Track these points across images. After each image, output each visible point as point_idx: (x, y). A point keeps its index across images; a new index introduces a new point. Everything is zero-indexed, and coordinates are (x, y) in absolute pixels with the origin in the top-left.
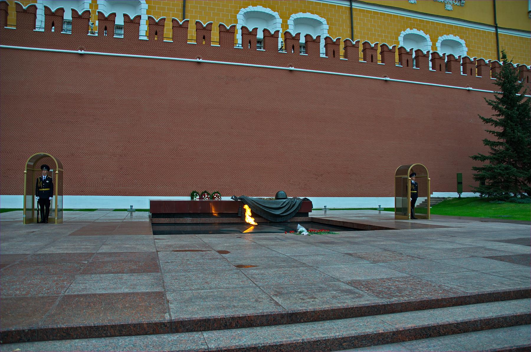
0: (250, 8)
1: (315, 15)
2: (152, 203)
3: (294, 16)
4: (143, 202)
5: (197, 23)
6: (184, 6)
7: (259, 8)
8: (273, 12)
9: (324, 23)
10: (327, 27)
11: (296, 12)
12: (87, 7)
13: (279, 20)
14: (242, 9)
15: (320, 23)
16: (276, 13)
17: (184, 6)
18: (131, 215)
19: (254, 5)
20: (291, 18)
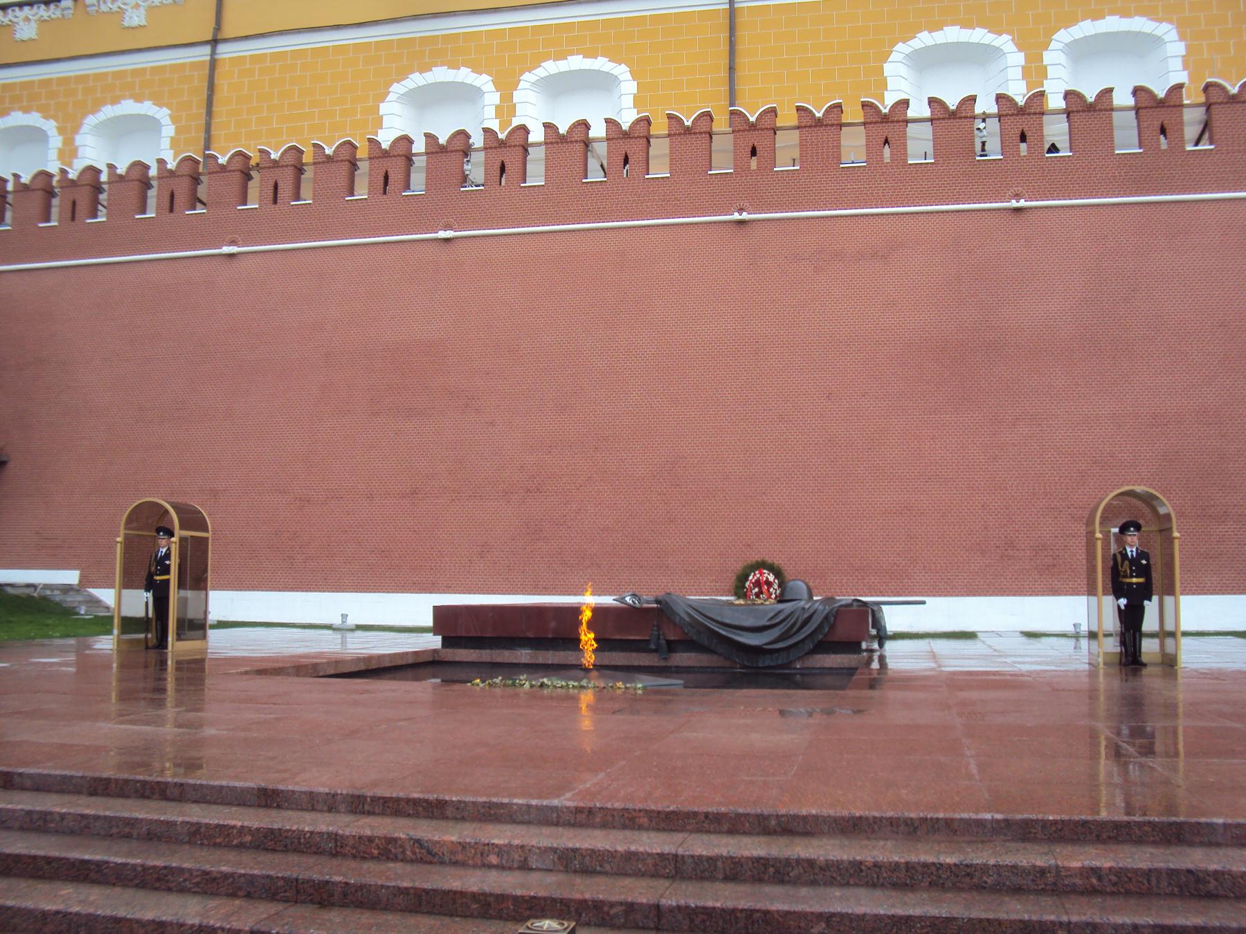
0: (924, 39)
1: (1137, 19)
3: (1063, 36)
6: (732, 69)
7: (952, 34)
8: (993, 36)
9: (1167, 38)
10: (1179, 48)
11: (1070, 21)
13: (1016, 59)
14: (900, 46)
15: (1156, 41)
16: (1006, 37)
17: (732, 69)
19: (935, 27)
20: (1053, 45)
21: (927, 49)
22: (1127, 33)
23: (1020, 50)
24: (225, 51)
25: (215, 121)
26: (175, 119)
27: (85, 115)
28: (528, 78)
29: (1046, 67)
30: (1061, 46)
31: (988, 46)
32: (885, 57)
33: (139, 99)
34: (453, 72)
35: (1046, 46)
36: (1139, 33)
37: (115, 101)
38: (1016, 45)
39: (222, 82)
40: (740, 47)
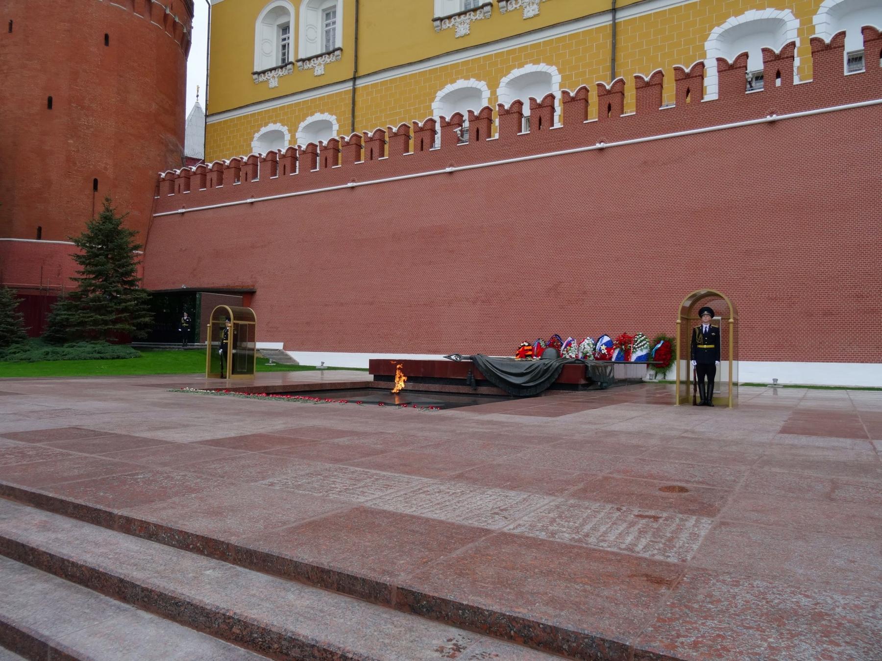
2: (372, 362)
4: (360, 360)
5: (636, 77)
6: (614, 60)
7: (751, 15)
12: (485, 104)
16: (787, 11)
17: (614, 60)
18: (322, 374)
21: (734, 28)
22: (761, 20)
23: (797, 18)
24: (360, 83)
25: (357, 120)
26: (338, 121)
27: (299, 123)
28: (505, 80)
29: (814, 26)
30: (826, 10)
31: (774, 20)
32: (705, 38)
33: (322, 112)
34: (466, 82)
35: (815, 12)
36: (768, 20)
37: (312, 114)
38: (794, 15)
39: (359, 99)
40: (618, 46)
